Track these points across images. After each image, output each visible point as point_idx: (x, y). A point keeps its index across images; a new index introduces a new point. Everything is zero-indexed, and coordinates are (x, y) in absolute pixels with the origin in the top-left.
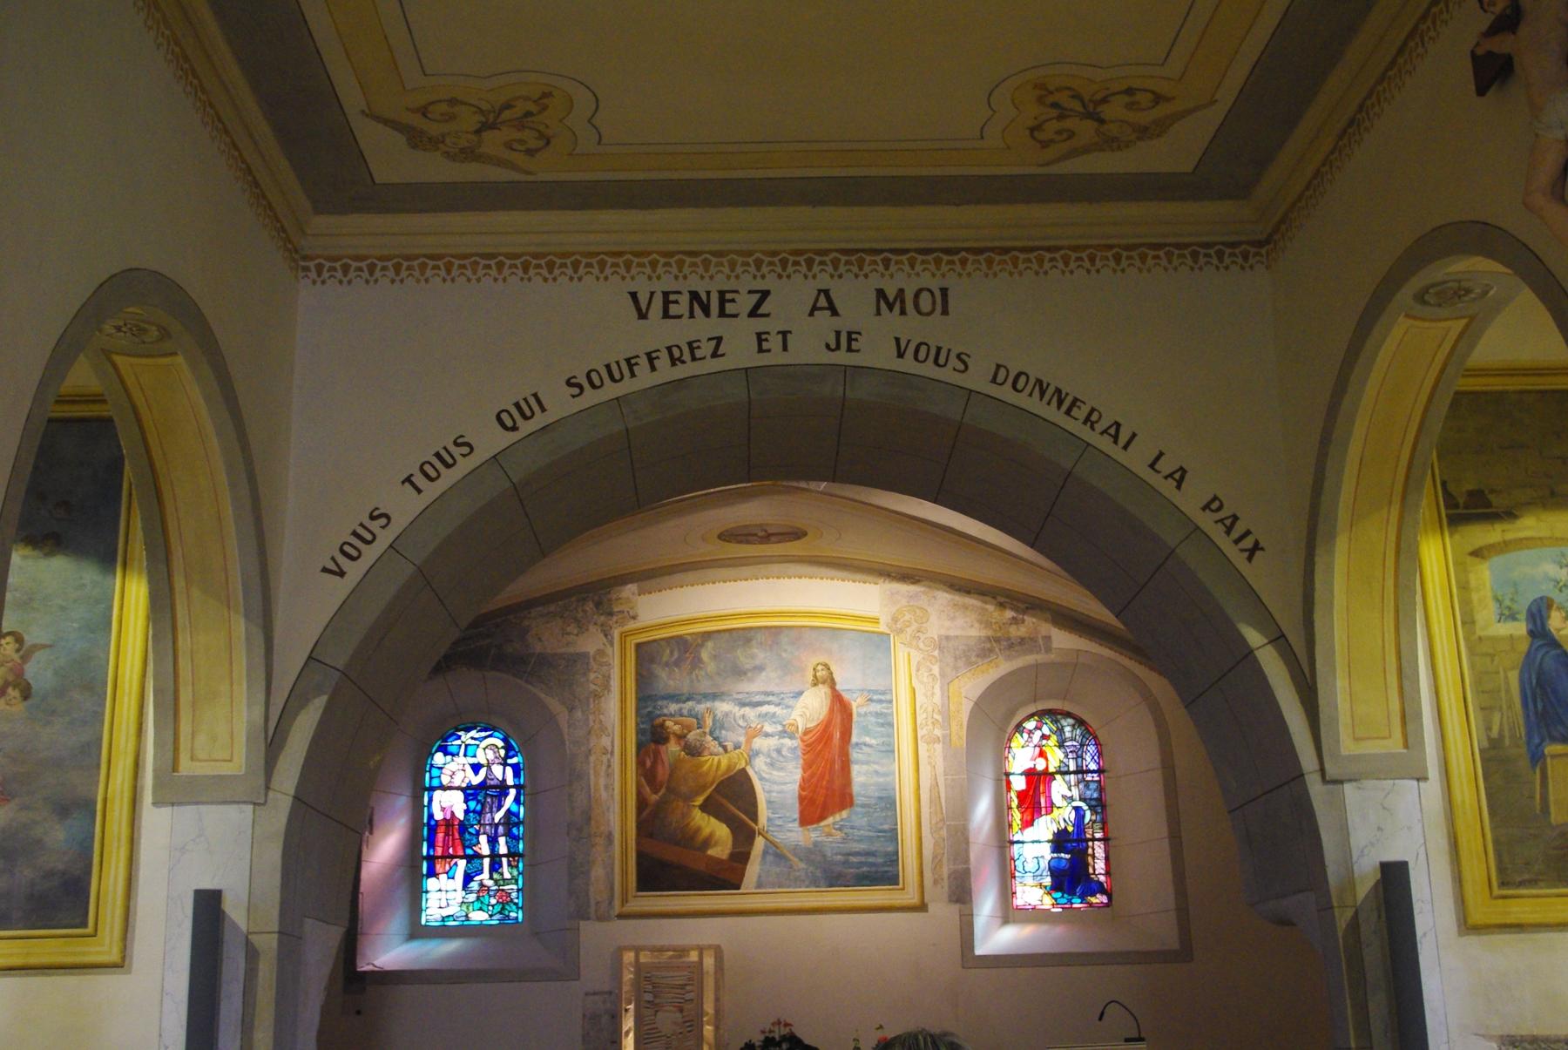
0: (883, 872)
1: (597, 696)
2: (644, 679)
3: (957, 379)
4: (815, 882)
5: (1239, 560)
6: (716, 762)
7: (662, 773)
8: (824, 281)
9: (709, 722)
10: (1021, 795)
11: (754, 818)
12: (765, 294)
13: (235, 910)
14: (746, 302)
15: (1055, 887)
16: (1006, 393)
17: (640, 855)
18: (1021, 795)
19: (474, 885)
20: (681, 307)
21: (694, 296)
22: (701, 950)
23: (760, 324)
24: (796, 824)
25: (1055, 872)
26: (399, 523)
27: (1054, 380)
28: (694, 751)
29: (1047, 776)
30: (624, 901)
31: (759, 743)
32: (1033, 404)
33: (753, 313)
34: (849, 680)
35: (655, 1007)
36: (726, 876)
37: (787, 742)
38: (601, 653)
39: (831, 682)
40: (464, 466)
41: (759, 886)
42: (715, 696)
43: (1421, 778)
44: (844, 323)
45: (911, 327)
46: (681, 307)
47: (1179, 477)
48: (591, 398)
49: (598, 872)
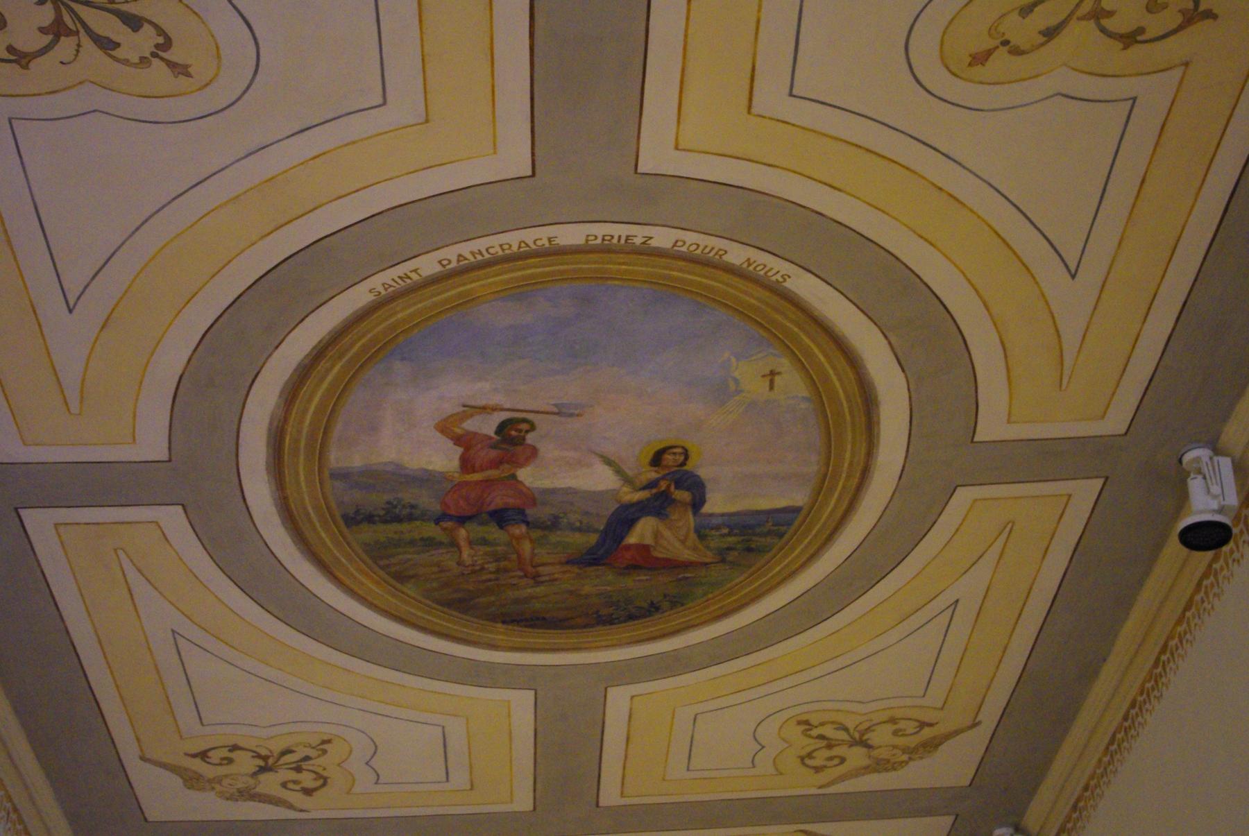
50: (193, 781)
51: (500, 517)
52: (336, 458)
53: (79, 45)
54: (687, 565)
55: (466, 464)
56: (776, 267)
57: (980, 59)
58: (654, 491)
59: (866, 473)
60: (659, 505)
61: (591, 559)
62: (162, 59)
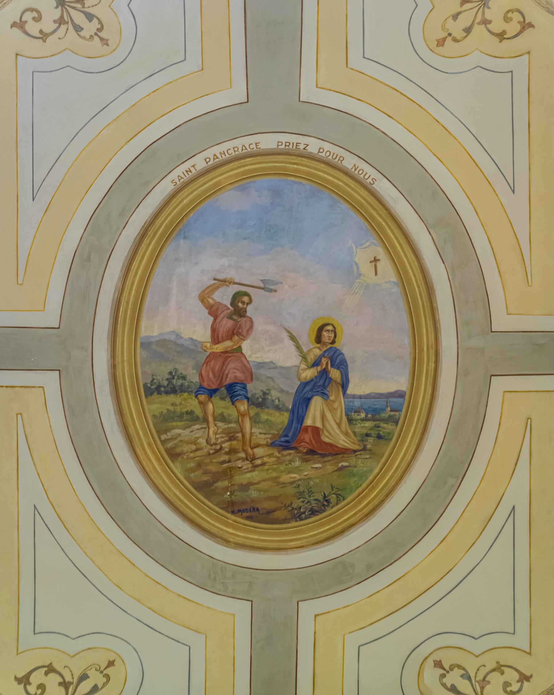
53: (67, 29)
54: (344, 452)
57: (441, 43)
58: (319, 368)
62: (98, 36)
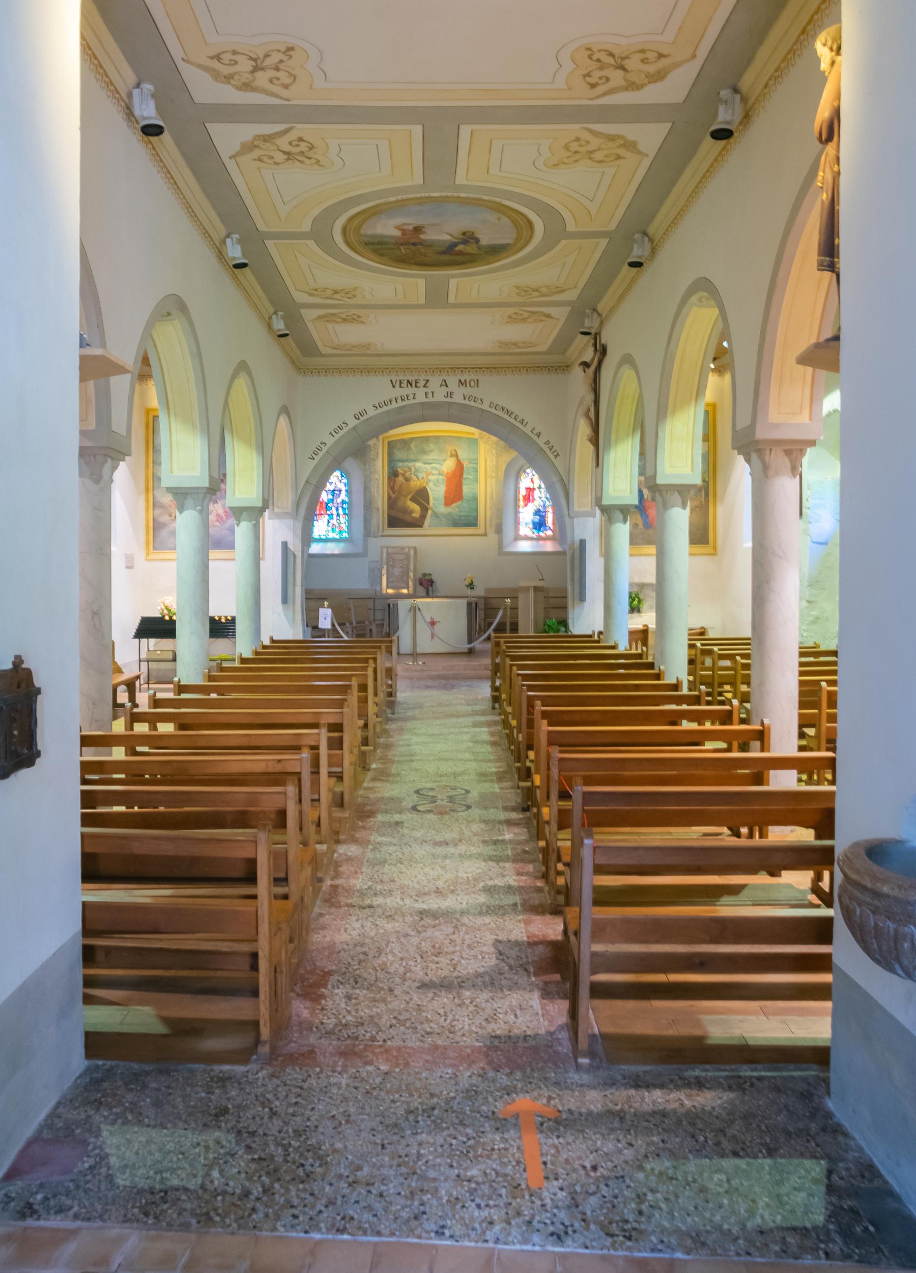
0: (472, 523)
1: (373, 460)
2: (390, 454)
3: (480, 406)
4: (449, 526)
5: (552, 458)
6: (415, 484)
7: (397, 487)
8: (444, 377)
9: (413, 470)
10: (524, 497)
11: (428, 501)
12: (428, 381)
13: (290, 546)
14: (422, 383)
15: (535, 528)
16: (493, 410)
17: (389, 516)
18: (524, 497)
19: (330, 524)
20: (405, 384)
21: (408, 381)
22: (409, 548)
23: (426, 390)
24: (442, 507)
25: (534, 523)
26: (328, 446)
27: (506, 407)
28: (408, 480)
29: (534, 489)
30: (383, 530)
31: (430, 477)
32: (500, 414)
33: (425, 386)
34: (462, 455)
35: (394, 567)
36: (417, 523)
37: (441, 477)
38: (375, 444)
39: (457, 456)
40: (346, 429)
41: (430, 526)
42: (415, 461)
43: (594, 516)
44: (449, 390)
45: (468, 391)
46: (405, 384)
47: (539, 435)
48: (380, 410)
49: (374, 521)
50: (311, 295)
51: (414, 244)
52: (362, 232)
55: (403, 234)
56: (498, 200)
59: (531, 237)
60: (465, 242)
61: (443, 253)
